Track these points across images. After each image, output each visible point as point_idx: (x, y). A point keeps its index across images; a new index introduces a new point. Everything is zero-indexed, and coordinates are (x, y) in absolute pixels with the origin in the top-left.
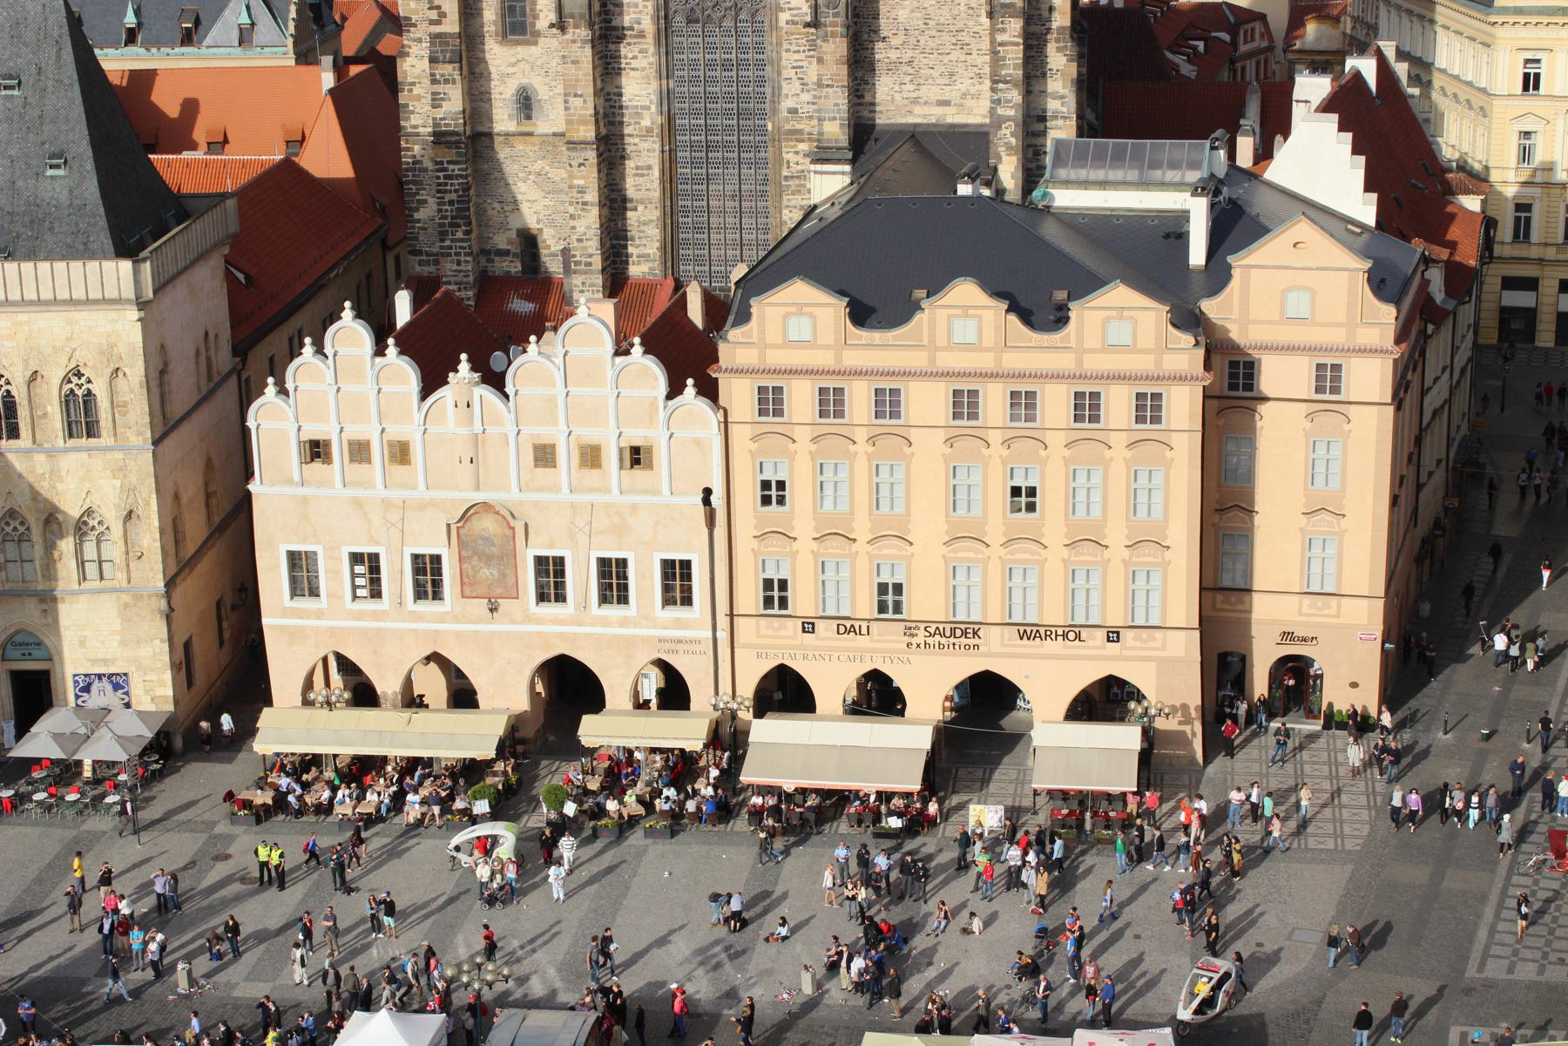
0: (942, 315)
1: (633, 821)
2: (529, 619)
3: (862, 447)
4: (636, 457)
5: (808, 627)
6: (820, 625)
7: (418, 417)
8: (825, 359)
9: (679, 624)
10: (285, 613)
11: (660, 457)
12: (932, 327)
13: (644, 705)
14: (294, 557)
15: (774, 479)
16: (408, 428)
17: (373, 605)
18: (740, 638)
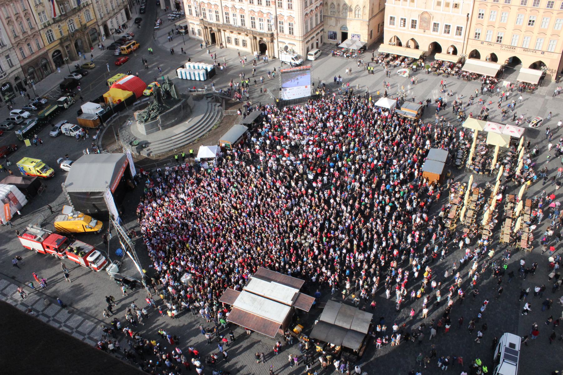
1: (441, 73)
2: (431, 34)
3: (501, 8)
4: (456, 6)
5: (482, 43)
11: (460, 7)
13: (449, 53)
14: (391, 18)
15: (481, 13)
17: (404, 28)
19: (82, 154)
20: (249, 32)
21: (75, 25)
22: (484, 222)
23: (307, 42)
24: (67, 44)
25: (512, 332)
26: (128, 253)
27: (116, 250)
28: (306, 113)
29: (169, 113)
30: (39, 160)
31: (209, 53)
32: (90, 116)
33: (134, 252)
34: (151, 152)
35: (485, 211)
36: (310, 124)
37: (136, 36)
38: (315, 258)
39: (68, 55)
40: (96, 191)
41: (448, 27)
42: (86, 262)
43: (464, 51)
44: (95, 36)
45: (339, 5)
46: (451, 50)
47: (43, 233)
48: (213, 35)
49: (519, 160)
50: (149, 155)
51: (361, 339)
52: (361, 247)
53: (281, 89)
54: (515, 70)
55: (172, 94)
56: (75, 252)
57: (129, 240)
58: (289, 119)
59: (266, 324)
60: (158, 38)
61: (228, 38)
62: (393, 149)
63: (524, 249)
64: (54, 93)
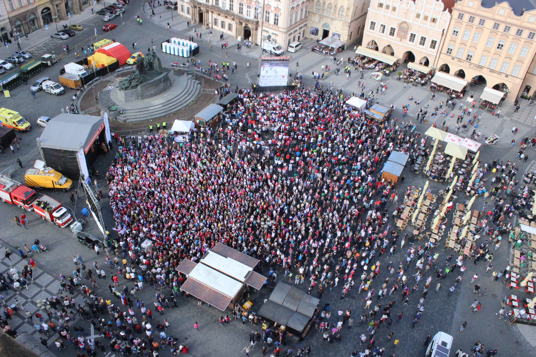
0: (498, 8)
1: (411, 82)
2: (406, 43)
3: (474, 29)
4: (434, 20)
5: (453, 59)
6: (455, 59)
7: (399, 4)
8: (473, 11)
9: (431, 52)
10: (368, 31)
12: (496, 10)
14: (372, 22)
15: (456, 30)
16: (397, 5)
18: (441, 57)
19: (61, 112)
20: (236, 17)
22: (433, 227)
23: (290, 35)
25: (446, 331)
26: (93, 213)
27: (82, 209)
29: (149, 84)
30: (16, 113)
31: (195, 31)
32: (72, 76)
33: (100, 213)
35: (436, 216)
38: (272, 240)
40: (69, 150)
41: (423, 40)
42: (52, 217)
43: (436, 64)
45: (324, 3)
46: (424, 61)
47: (12, 183)
48: (201, 15)
49: (473, 172)
50: (125, 121)
51: (305, 323)
52: (316, 235)
53: (259, 76)
55: (154, 65)
56: (42, 206)
57: (97, 201)
58: (263, 105)
59: (218, 296)
62: (358, 146)
63: (466, 255)
64: (40, 48)
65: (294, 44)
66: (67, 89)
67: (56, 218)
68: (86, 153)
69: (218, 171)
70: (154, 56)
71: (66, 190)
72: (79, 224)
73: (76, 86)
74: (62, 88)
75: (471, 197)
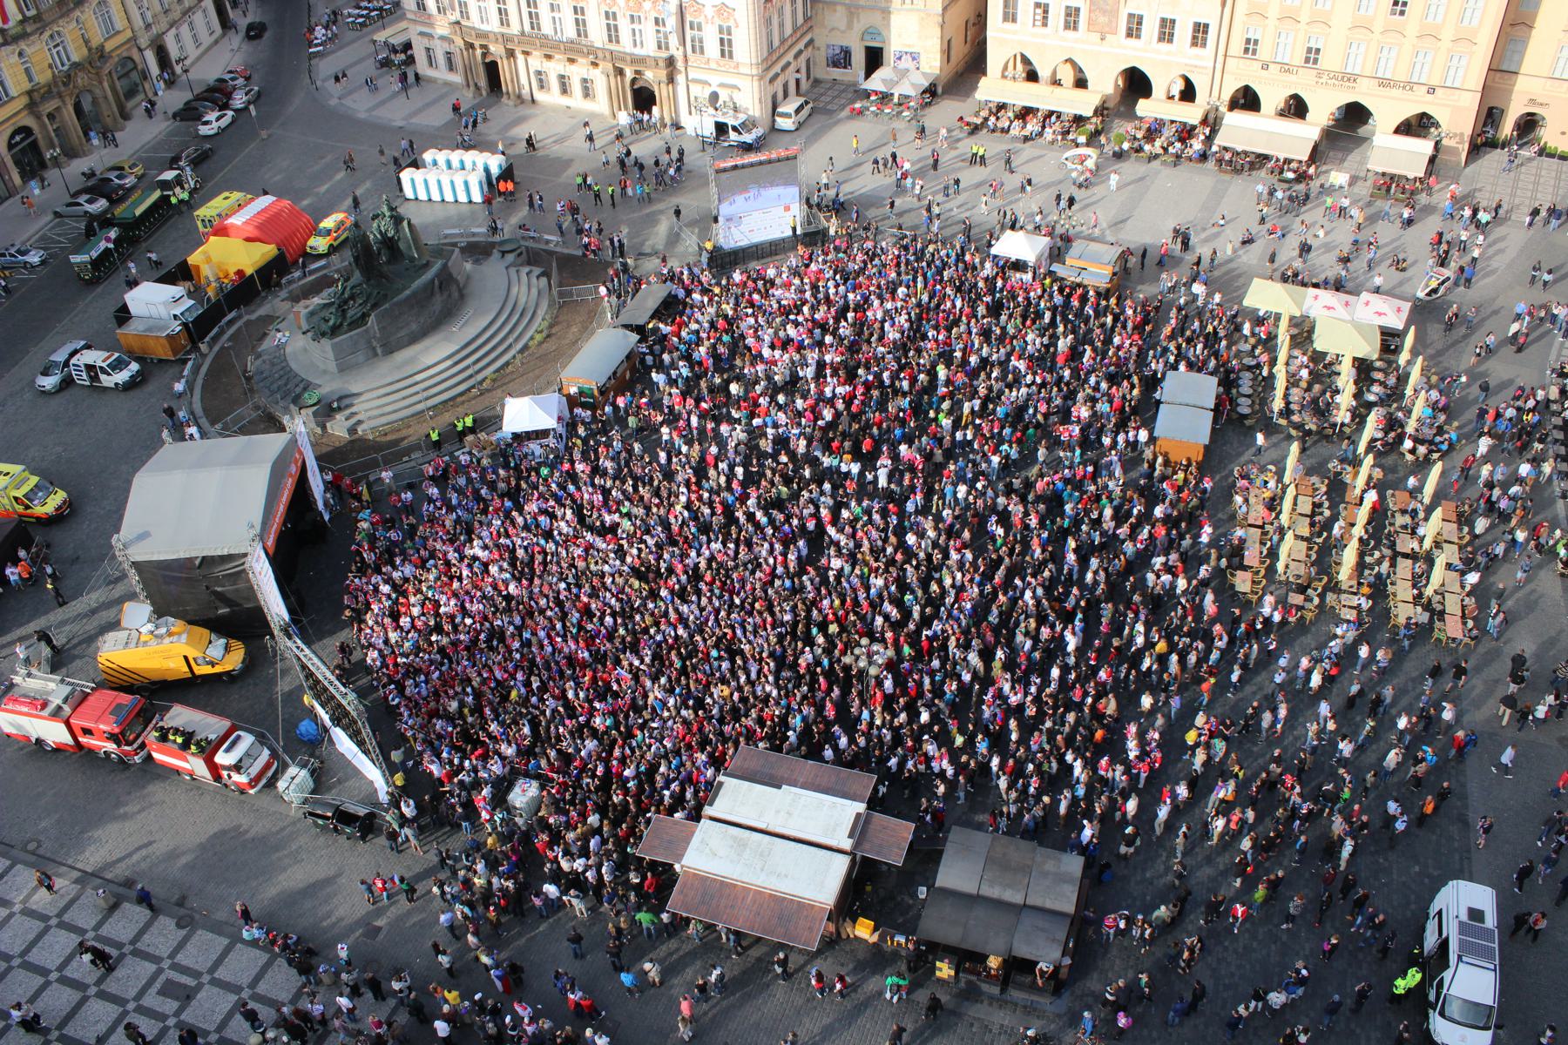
1: (1156, 156)
5: (1265, 67)
13: (1171, 98)
17: (1044, 30)
19: (163, 443)
20: (600, 54)
21: (71, 48)
22: (1345, 574)
23: (772, 80)
24: (49, 106)
27: (296, 726)
28: (797, 281)
29: (399, 304)
30: (15, 469)
32: (155, 324)
33: (366, 732)
34: (360, 422)
36: (817, 316)
37: (255, 77)
39: (56, 140)
42: (215, 769)
44: (131, 82)
46: (1176, 91)
47: (69, 688)
48: (492, 69)
49: (1409, 392)
50: (352, 430)
51: (1062, 935)
53: (716, 220)
54: (1364, 140)
55: (402, 246)
56: (179, 740)
57: (352, 696)
58: (752, 304)
59: (787, 908)
60: (324, 81)
61: (539, 73)
65: (789, 107)
66: (151, 367)
67: (228, 768)
68: (271, 552)
69: (675, 528)
70: (397, 220)
71: (227, 679)
72: (304, 773)
73: (175, 353)
74: (134, 366)
75: (1423, 465)
